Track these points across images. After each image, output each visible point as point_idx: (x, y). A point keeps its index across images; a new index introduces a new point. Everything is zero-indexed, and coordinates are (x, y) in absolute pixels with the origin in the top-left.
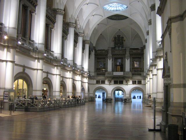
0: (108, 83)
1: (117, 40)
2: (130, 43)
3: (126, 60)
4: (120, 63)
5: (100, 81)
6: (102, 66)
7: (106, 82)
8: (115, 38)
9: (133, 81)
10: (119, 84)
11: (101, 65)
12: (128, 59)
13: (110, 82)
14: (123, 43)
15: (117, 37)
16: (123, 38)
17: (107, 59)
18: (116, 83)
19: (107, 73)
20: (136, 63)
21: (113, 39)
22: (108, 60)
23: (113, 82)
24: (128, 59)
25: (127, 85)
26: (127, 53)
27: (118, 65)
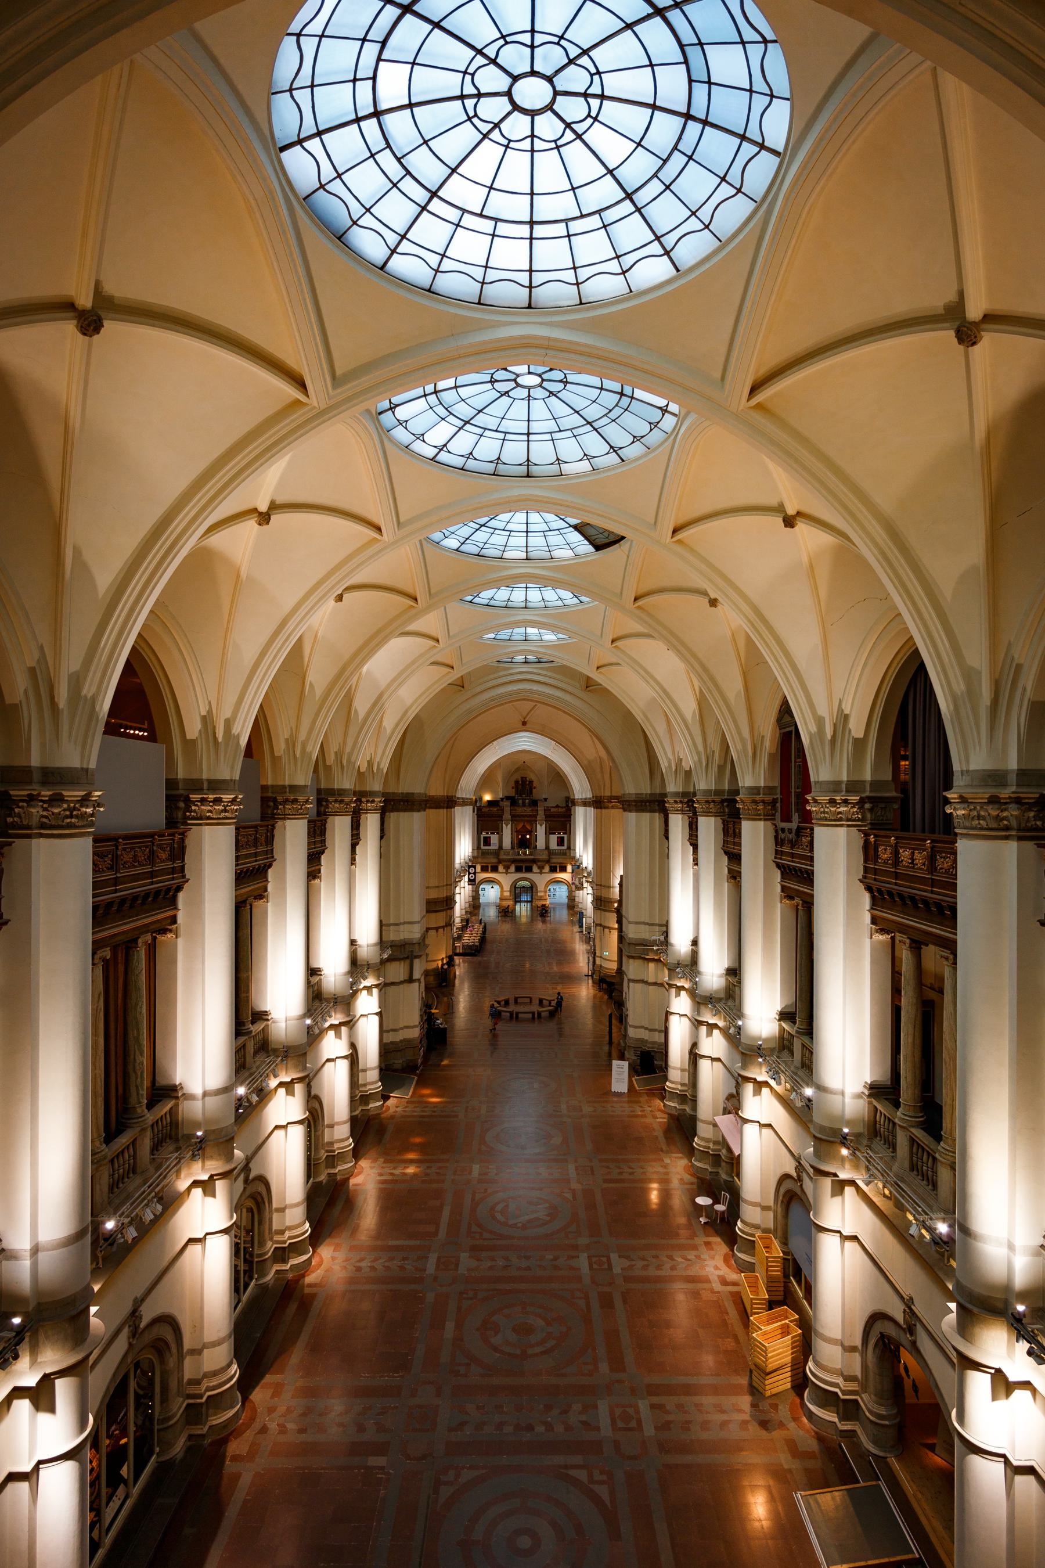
1: (520, 787)
2: (542, 791)
3: (538, 826)
7: (501, 868)
8: (517, 782)
9: (551, 867)
12: (541, 825)
13: (507, 868)
14: (531, 793)
15: (520, 779)
16: (531, 782)
18: (518, 870)
19: (502, 852)
21: (513, 783)
23: (513, 868)
24: (541, 825)
25: (541, 873)
26: (539, 812)
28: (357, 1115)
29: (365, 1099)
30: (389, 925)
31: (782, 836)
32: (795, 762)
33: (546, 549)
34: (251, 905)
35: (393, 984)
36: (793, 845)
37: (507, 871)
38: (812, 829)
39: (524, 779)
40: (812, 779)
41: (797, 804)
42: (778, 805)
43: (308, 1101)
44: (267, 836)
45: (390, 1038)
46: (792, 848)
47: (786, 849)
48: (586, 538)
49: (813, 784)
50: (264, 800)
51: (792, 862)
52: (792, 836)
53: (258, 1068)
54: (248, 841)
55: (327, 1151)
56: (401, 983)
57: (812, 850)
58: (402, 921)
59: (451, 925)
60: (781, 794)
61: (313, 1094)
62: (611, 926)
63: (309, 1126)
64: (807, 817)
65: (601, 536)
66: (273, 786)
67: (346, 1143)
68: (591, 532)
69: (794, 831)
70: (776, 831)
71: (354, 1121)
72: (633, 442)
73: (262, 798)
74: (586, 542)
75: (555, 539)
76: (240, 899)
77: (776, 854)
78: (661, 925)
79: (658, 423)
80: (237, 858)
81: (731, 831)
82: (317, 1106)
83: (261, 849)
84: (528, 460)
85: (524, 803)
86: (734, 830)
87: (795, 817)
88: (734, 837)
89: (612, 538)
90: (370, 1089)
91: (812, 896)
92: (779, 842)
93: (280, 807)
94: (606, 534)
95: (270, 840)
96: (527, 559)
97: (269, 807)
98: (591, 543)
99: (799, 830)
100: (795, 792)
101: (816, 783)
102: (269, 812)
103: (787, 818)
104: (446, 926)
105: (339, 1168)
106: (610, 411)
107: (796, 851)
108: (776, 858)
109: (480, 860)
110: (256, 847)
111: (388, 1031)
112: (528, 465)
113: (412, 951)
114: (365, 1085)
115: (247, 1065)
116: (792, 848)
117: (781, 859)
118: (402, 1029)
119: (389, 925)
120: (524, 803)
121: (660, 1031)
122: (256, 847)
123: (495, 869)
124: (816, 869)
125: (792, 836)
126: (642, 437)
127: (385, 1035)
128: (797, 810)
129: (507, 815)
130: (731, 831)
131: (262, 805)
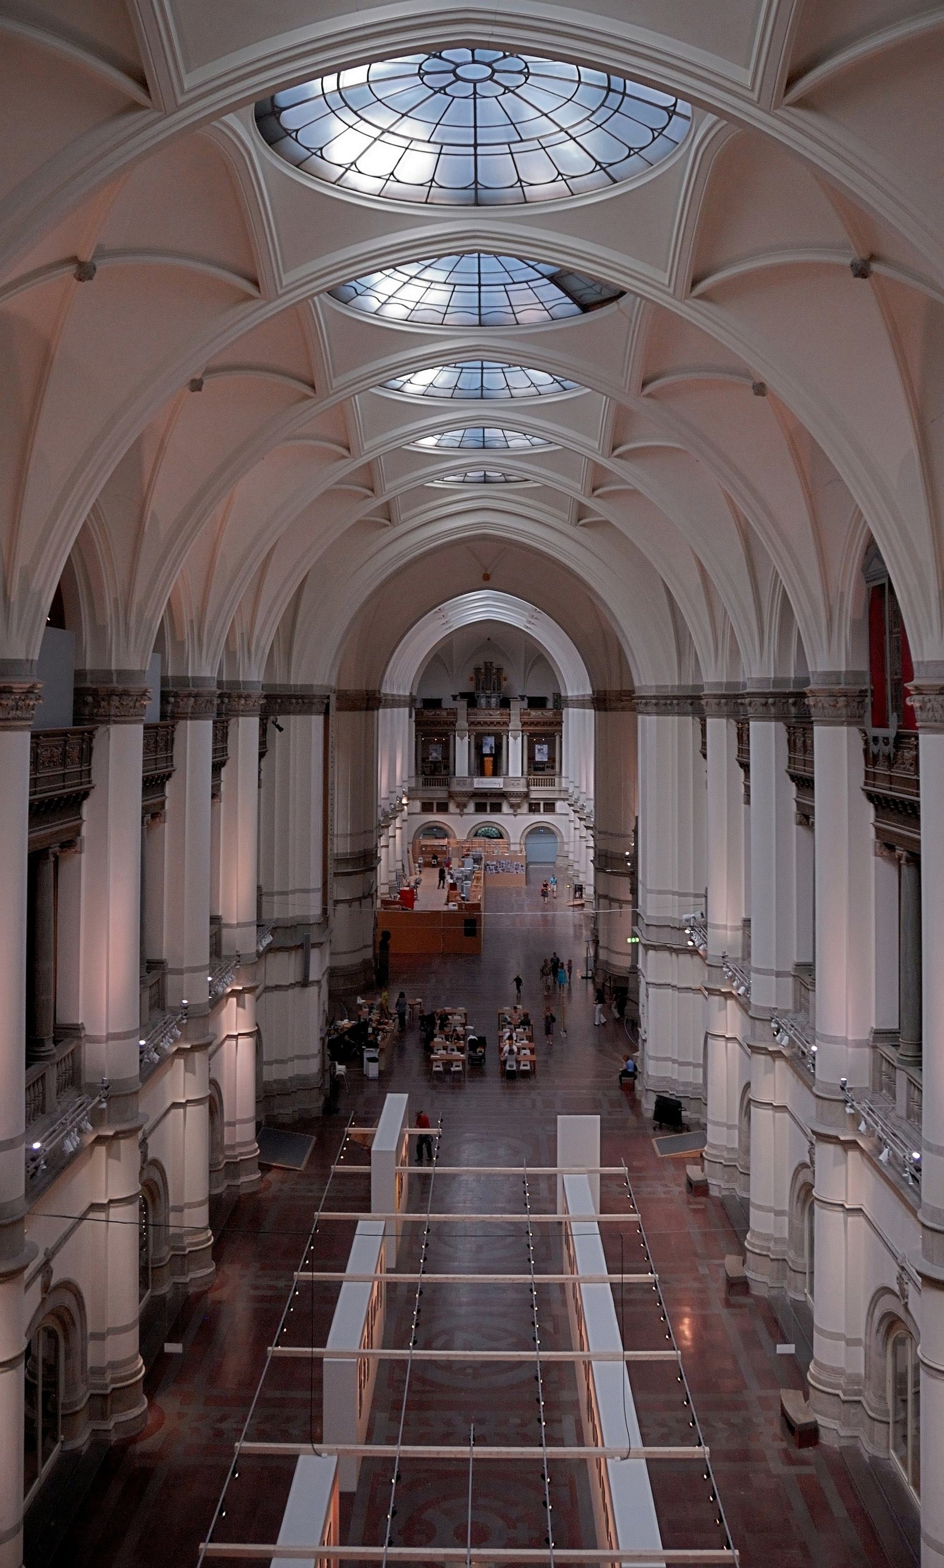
0: (458, 811)
4: (491, 748)
5: (432, 803)
6: (436, 758)
7: (452, 808)
8: (477, 670)
10: (489, 814)
11: (434, 755)
13: (462, 806)
15: (482, 666)
17: (455, 736)
20: (539, 750)
22: (457, 738)
23: (471, 808)
26: (512, 718)
27: (487, 755)
28: (221, 1194)
29: (234, 1168)
30: (272, 894)
31: (873, 748)
32: (891, 632)
33: (509, 310)
34: (57, 858)
35: (278, 987)
36: (891, 762)
37: (462, 810)
38: (917, 738)
39: (488, 666)
40: (914, 659)
41: (895, 698)
42: (868, 700)
43: (142, 1168)
44: (82, 749)
45: (272, 1074)
46: (890, 767)
47: (881, 769)
48: (568, 294)
49: (915, 666)
50: (79, 694)
51: (891, 789)
52: (889, 749)
53: (64, 1112)
54: (52, 756)
55: (173, 1248)
56: (292, 986)
57: (917, 772)
58: (291, 888)
59: (370, 895)
60: (872, 682)
61: (150, 1156)
62: (622, 898)
63: (144, 1208)
64: (908, 718)
65: (589, 291)
66: (93, 672)
67: (203, 1237)
68: (574, 284)
69: (891, 741)
70: (866, 742)
71: (215, 1203)
72: (629, 156)
73: (76, 690)
74: (568, 300)
75: (521, 296)
76: (39, 847)
77: (867, 777)
78: (697, 896)
79: (664, 128)
80: (34, 782)
81: (799, 743)
82: (157, 1177)
83: (73, 768)
84: (476, 182)
85: (488, 703)
86: (804, 742)
87: (893, 719)
88: (805, 752)
89: (607, 294)
90: (241, 1154)
91: (918, 842)
92: (871, 759)
93: (103, 703)
94: (597, 288)
95: (86, 755)
96: (480, 325)
97: (86, 703)
98: (575, 301)
99: (899, 737)
100: (892, 680)
101: (918, 663)
102: (87, 712)
103: (880, 721)
104: (365, 897)
105: (192, 1275)
106: (594, 112)
107: (896, 773)
108: (866, 784)
109: (420, 794)
110: (64, 765)
111: (270, 1063)
112: (476, 189)
113: (308, 937)
114: (232, 1147)
115: (48, 1110)
116: (890, 767)
117: (874, 786)
118: (291, 1059)
119: (272, 894)
120: (488, 703)
121: (696, 1066)
122: (64, 765)
123: (443, 808)
124: (922, 800)
125: (889, 749)
126: (642, 149)
127: (265, 1068)
128: (895, 708)
129: (462, 723)
130: (799, 743)
131: (75, 702)
